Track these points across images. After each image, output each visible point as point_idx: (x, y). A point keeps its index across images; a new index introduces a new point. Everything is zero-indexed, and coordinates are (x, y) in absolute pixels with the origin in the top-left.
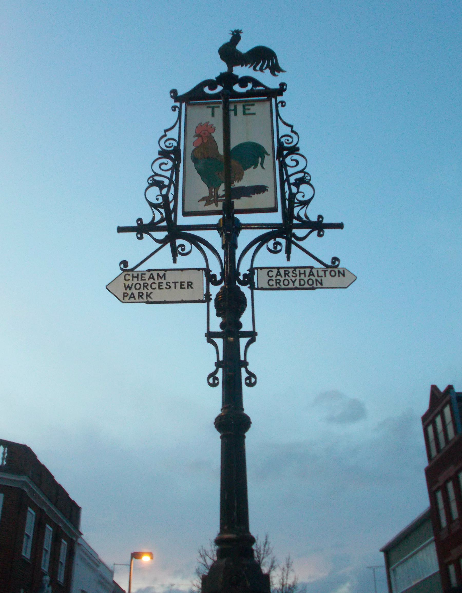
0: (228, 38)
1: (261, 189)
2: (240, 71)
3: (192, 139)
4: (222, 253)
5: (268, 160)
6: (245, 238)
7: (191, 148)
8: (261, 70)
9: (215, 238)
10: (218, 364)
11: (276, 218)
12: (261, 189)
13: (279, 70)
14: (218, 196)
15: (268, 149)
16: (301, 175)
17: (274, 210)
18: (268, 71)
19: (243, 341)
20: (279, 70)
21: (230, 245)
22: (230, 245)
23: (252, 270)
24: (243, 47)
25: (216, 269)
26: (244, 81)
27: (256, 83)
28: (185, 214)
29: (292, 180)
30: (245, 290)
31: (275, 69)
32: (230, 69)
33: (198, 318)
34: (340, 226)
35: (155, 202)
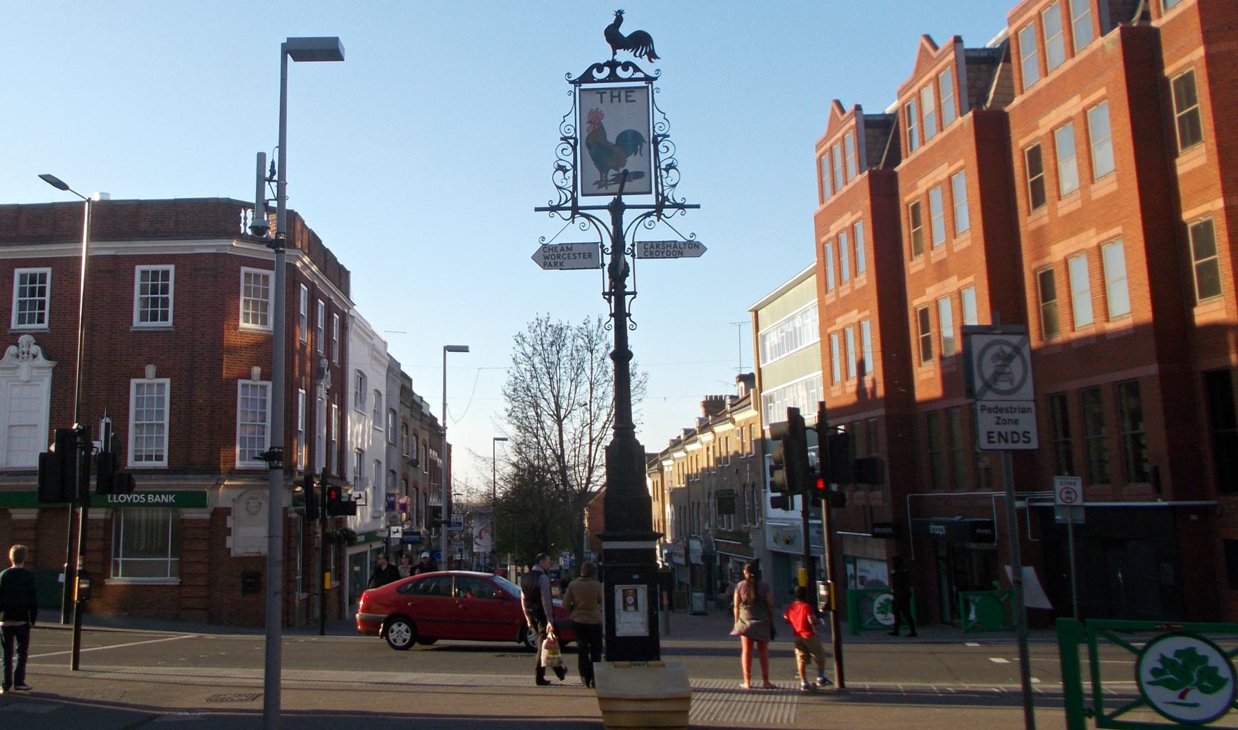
0: (611, 20)
1: (639, 175)
2: (624, 55)
3: (586, 126)
4: (611, 228)
5: (645, 145)
6: (628, 216)
7: (586, 134)
8: (640, 56)
9: (606, 216)
10: (611, 315)
11: (650, 199)
12: (639, 175)
13: (656, 57)
14: (607, 180)
15: (644, 135)
16: (669, 161)
17: (650, 193)
18: (646, 57)
19: (628, 298)
20: (656, 57)
21: (617, 222)
22: (617, 222)
23: (633, 245)
24: (625, 31)
25: (608, 243)
26: (626, 66)
27: (637, 69)
28: (583, 195)
29: (663, 166)
30: (629, 259)
31: (652, 55)
32: (615, 54)
33: (596, 280)
34: (698, 207)
35: (560, 185)
